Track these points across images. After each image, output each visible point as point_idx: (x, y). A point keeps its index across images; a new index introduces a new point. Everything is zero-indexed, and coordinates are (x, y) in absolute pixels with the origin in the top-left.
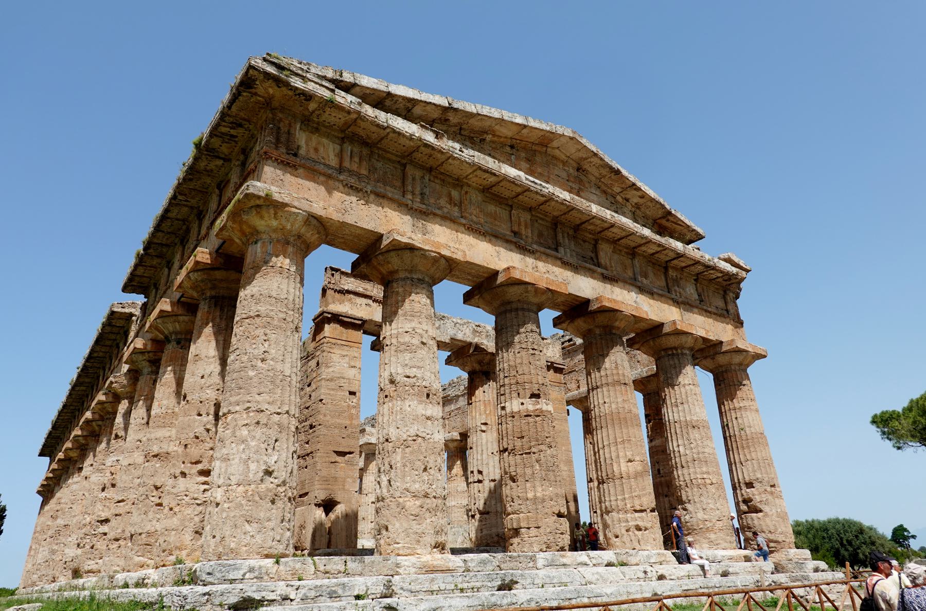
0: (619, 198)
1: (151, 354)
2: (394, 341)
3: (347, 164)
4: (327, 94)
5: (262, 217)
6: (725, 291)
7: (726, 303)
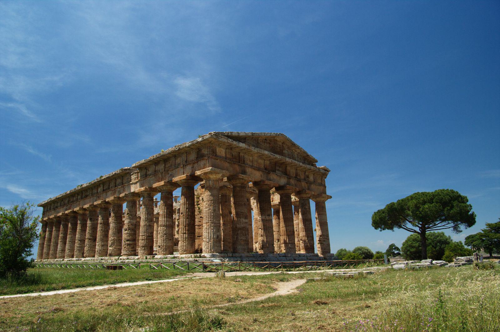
0: (294, 150)
1: (148, 192)
2: (238, 203)
3: (227, 156)
4: (226, 141)
5: (212, 175)
6: (322, 177)
7: (322, 181)
